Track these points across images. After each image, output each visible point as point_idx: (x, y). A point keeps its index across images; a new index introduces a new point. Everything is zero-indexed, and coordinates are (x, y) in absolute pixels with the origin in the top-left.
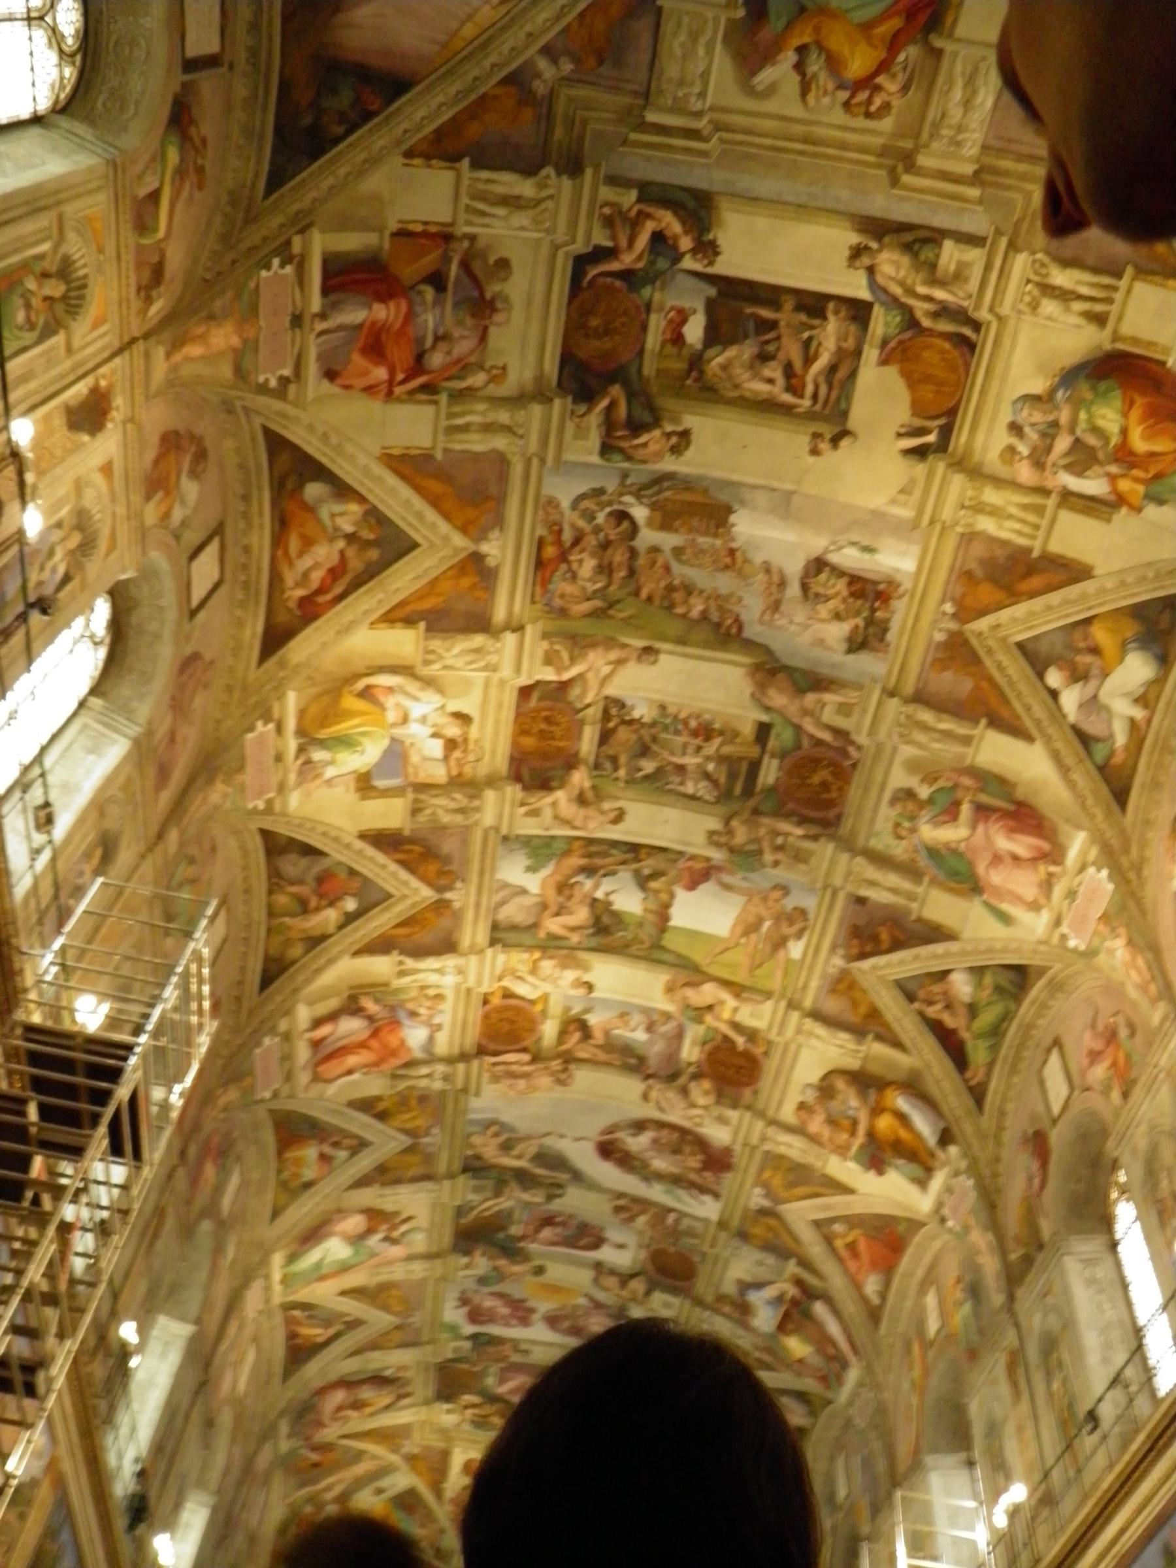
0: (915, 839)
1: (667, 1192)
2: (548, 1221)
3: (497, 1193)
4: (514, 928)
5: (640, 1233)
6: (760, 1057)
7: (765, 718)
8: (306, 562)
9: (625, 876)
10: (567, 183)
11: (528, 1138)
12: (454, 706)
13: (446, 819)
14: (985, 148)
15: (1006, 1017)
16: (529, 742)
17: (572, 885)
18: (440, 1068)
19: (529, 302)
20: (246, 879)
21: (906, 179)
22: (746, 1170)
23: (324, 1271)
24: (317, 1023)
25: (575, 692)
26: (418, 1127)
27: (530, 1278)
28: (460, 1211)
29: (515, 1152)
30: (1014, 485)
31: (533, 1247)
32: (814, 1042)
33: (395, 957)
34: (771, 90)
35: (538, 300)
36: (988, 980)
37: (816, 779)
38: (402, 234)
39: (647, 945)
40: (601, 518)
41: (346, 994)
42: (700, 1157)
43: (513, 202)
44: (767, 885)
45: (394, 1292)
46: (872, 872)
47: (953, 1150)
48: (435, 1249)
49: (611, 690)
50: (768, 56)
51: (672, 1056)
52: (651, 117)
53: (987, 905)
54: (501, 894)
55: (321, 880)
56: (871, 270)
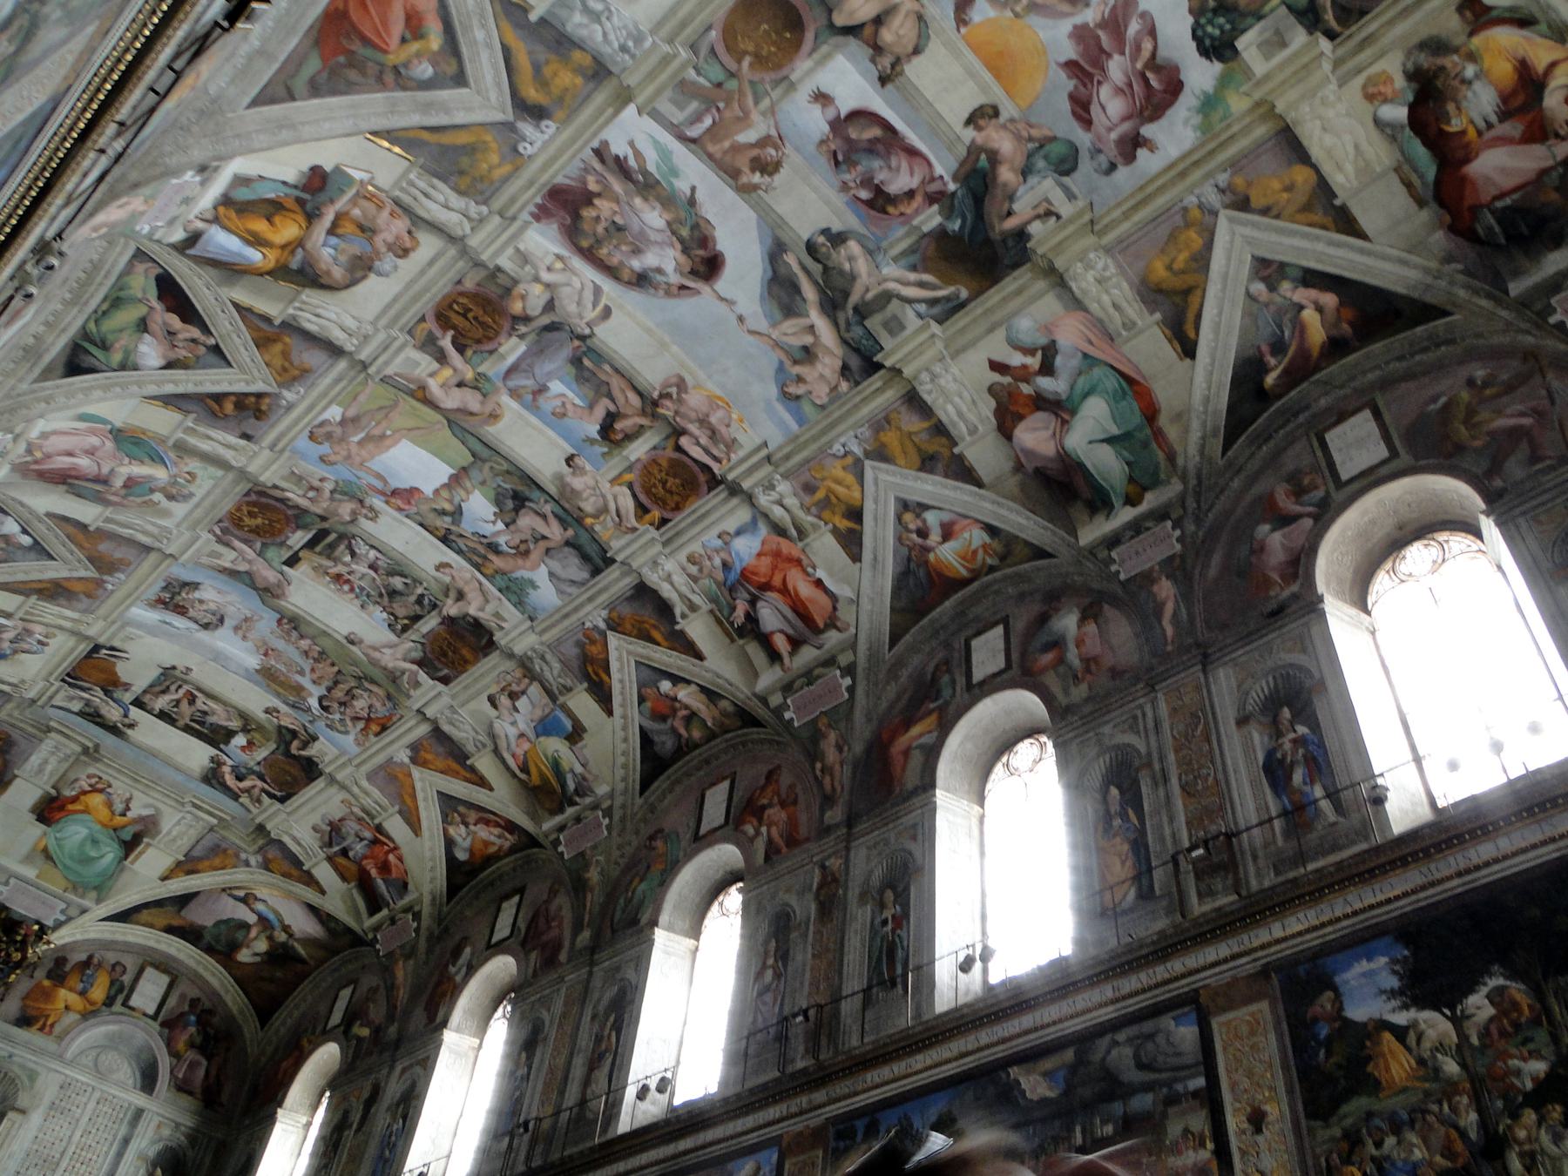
0: (174, 471)
1: (674, 172)
2: (880, 202)
3: (887, 297)
4: (585, 558)
5: (772, 111)
6: (430, 318)
7: (285, 568)
8: (493, 838)
9: (467, 527)
10: (269, 827)
11: (777, 344)
12: (493, 713)
13: (557, 666)
14: (41, 740)
15: (100, 315)
16: (465, 652)
17: (517, 548)
18: (763, 500)
19: (313, 810)
20: (699, 769)
21: (90, 745)
22: (531, 183)
23: (1137, 418)
24: (774, 656)
25: (417, 655)
26: (844, 468)
27: (1008, 110)
28: (948, 310)
29: (808, 340)
30: (46, 625)
31: (944, 167)
32: (351, 323)
33: (682, 625)
34: (147, 806)
35: (309, 806)
36: (116, 358)
37: (259, 521)
38: (344, 878)
39: (487, 466)
40: (337, 716)
41: (741, 642)
42: (588, 213)
43: (294, 839)
44: (339, 467)
45: (1160, 271)
46: (228, 455)
47: (178, 235)
48: (1041, 284)
49: (392, 637)
50: (141, 819)
51: (538, 351)
52: (215, 821)
53: (104, 422)
54: (569, 590)
55: (663, 718)
56: (126, 716)
